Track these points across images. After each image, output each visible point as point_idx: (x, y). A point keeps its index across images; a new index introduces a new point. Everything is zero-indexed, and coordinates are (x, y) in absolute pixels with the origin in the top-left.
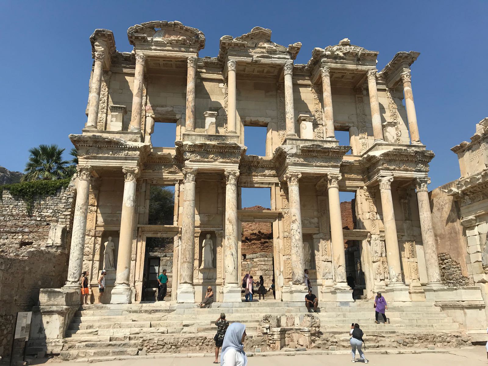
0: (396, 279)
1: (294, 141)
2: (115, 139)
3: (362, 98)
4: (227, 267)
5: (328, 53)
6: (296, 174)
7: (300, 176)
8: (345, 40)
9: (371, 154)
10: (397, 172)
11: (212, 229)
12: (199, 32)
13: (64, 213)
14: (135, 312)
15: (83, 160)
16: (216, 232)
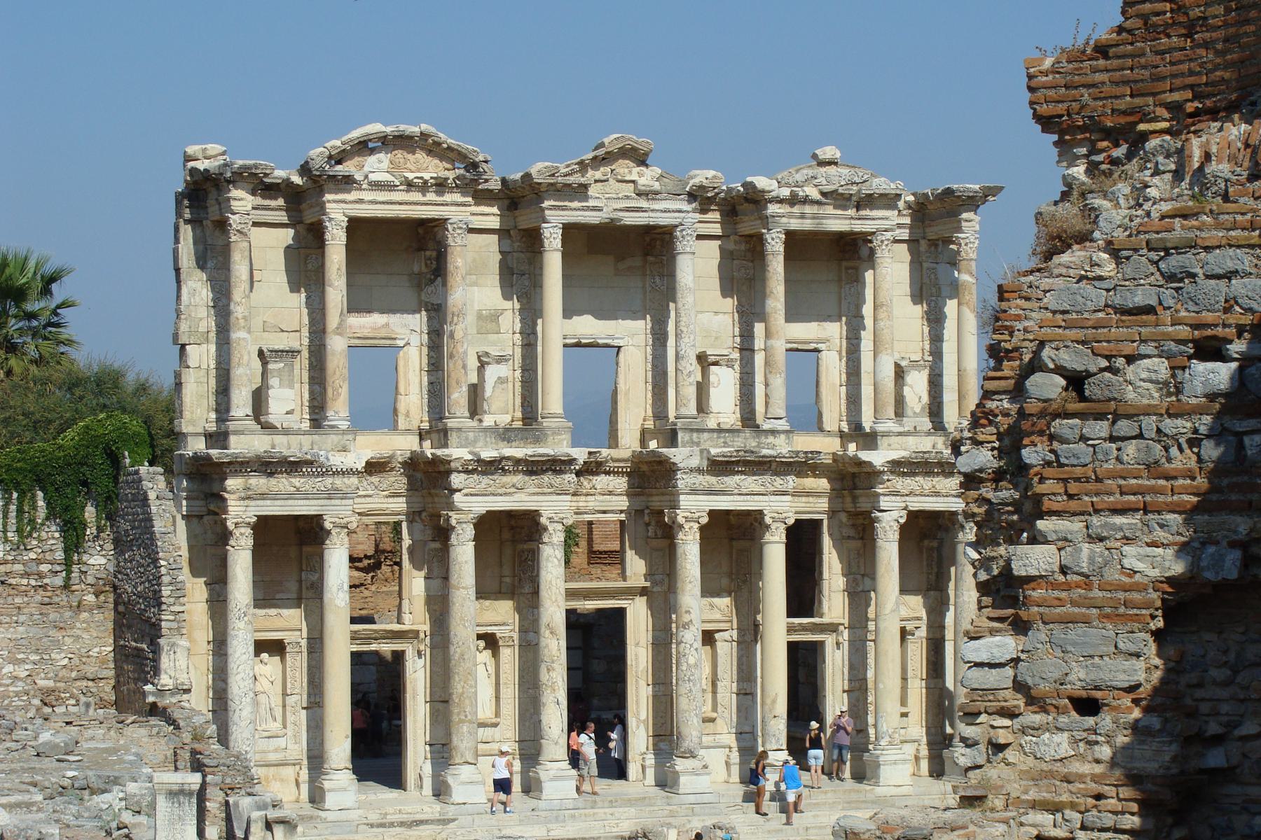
0: (887, 739)
1: (695, 435)
2: (309, 457)
3: (856, 269)
4: (546, 728)
5: (786, 192)
6: (697, 515)
7: (705, 520)
8: (828, 152)
9: (865, 456)
10: (916, 499)
11: (489, 630)
12: (481, 158)
13: (172, 608)
14: (382, 825)
15: (238, 503)
16: (498, 635)
